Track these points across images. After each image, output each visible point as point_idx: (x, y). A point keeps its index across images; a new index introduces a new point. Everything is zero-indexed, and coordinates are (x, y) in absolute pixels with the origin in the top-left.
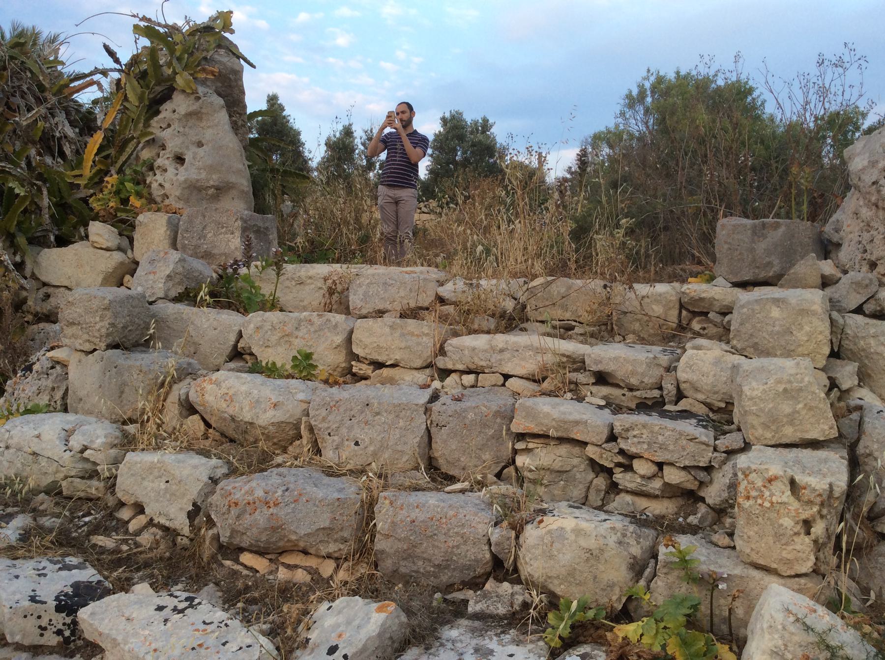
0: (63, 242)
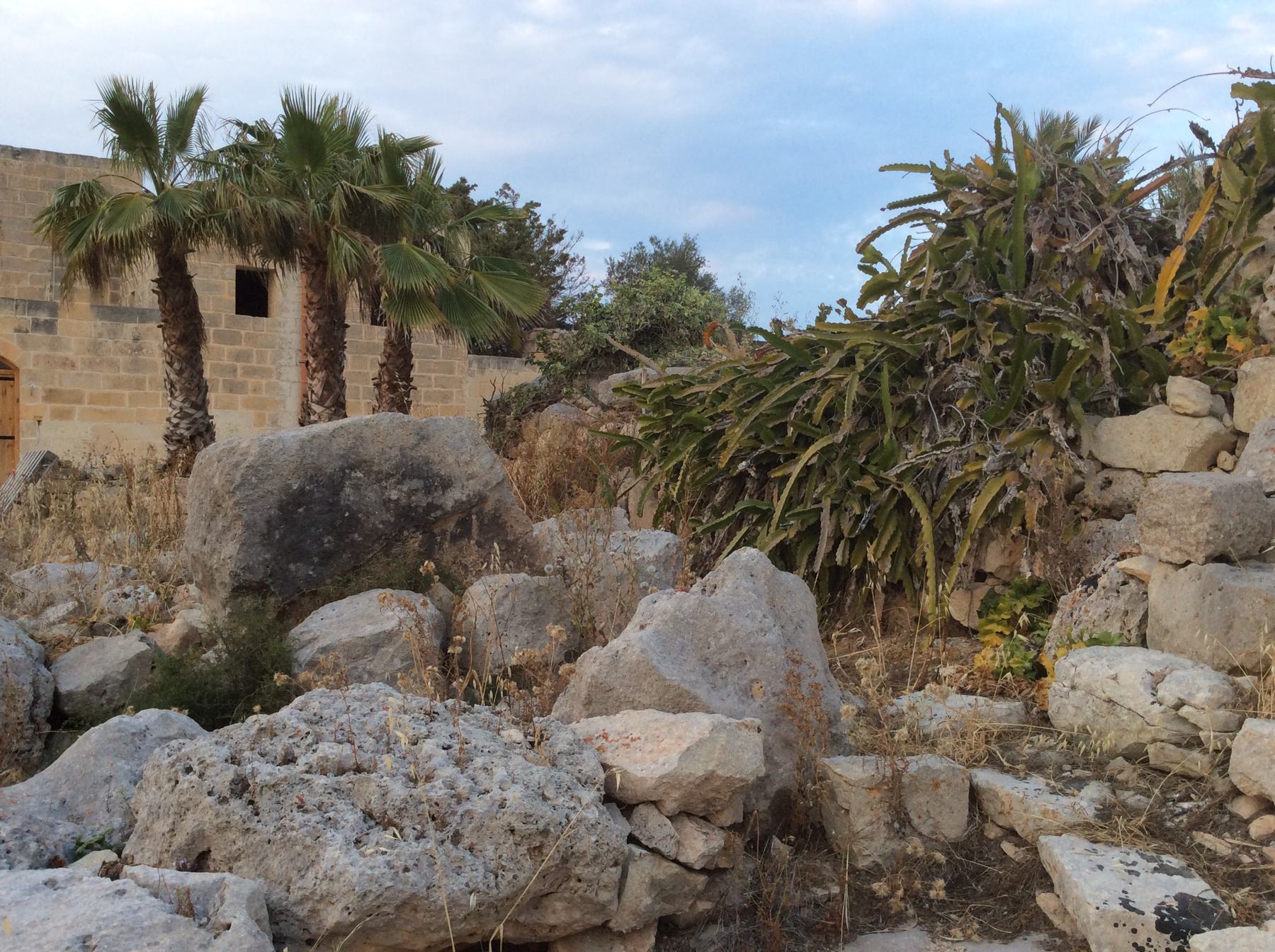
0: (1129, 407)
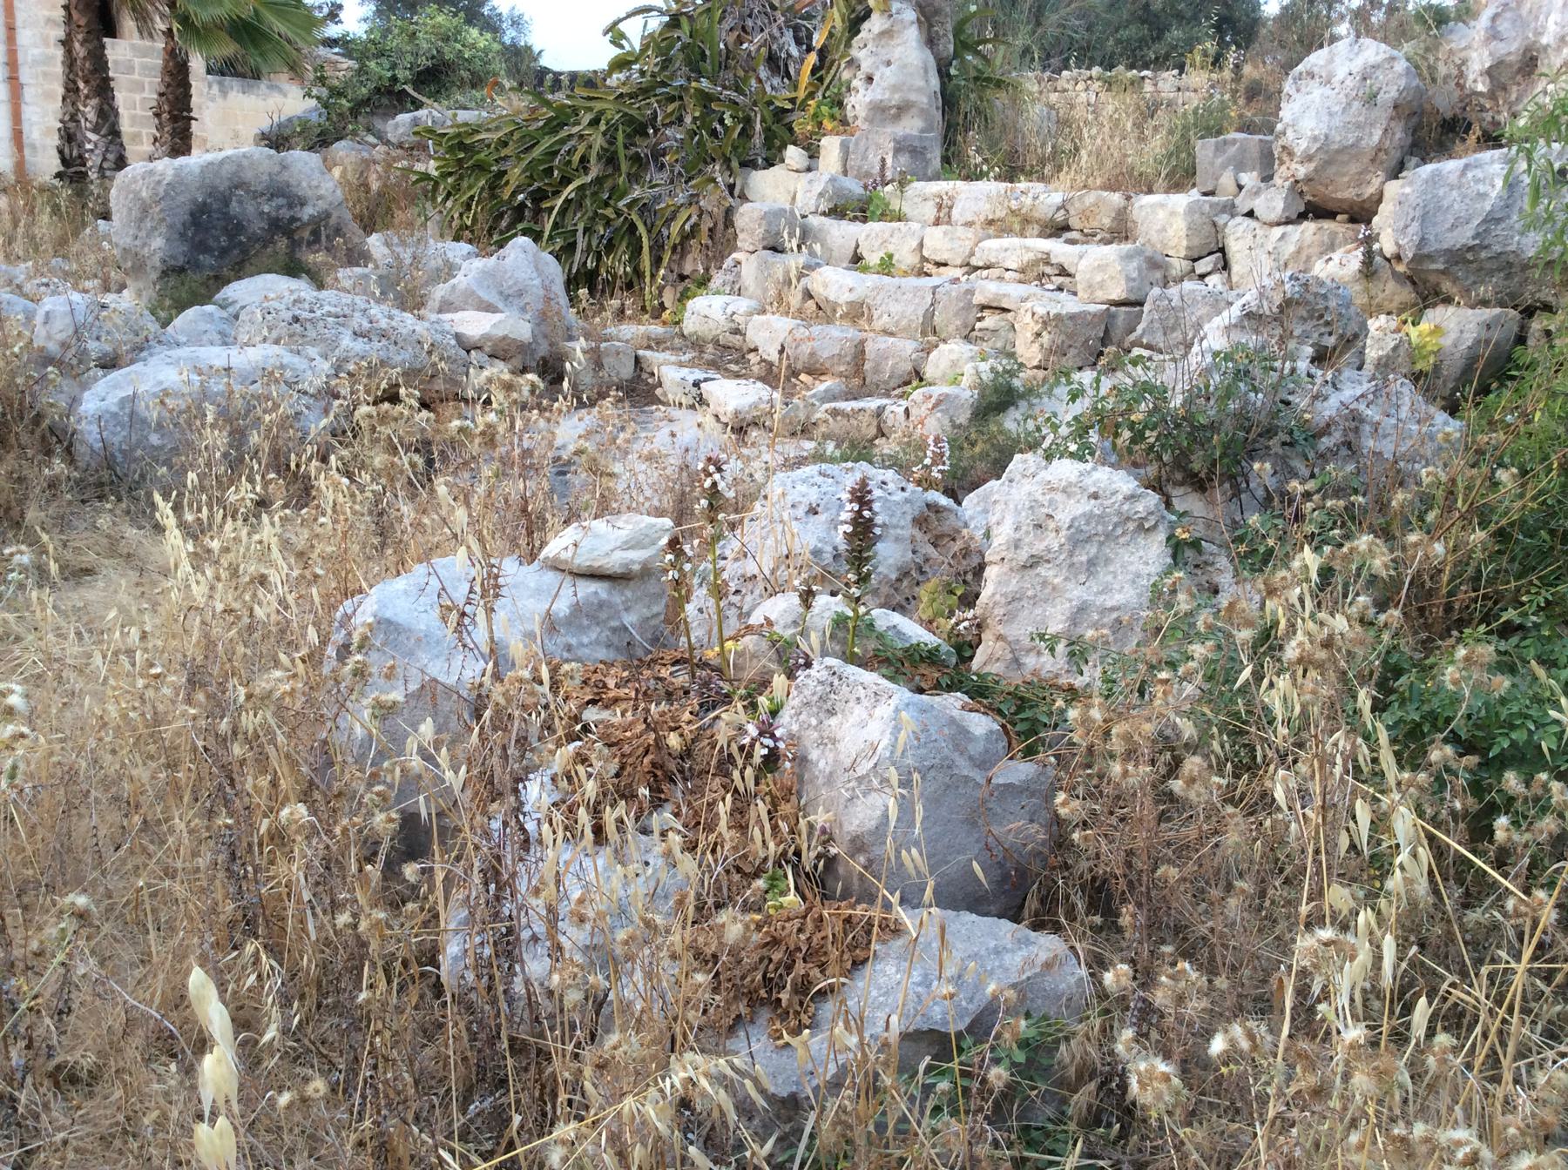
0: (769, 163)
